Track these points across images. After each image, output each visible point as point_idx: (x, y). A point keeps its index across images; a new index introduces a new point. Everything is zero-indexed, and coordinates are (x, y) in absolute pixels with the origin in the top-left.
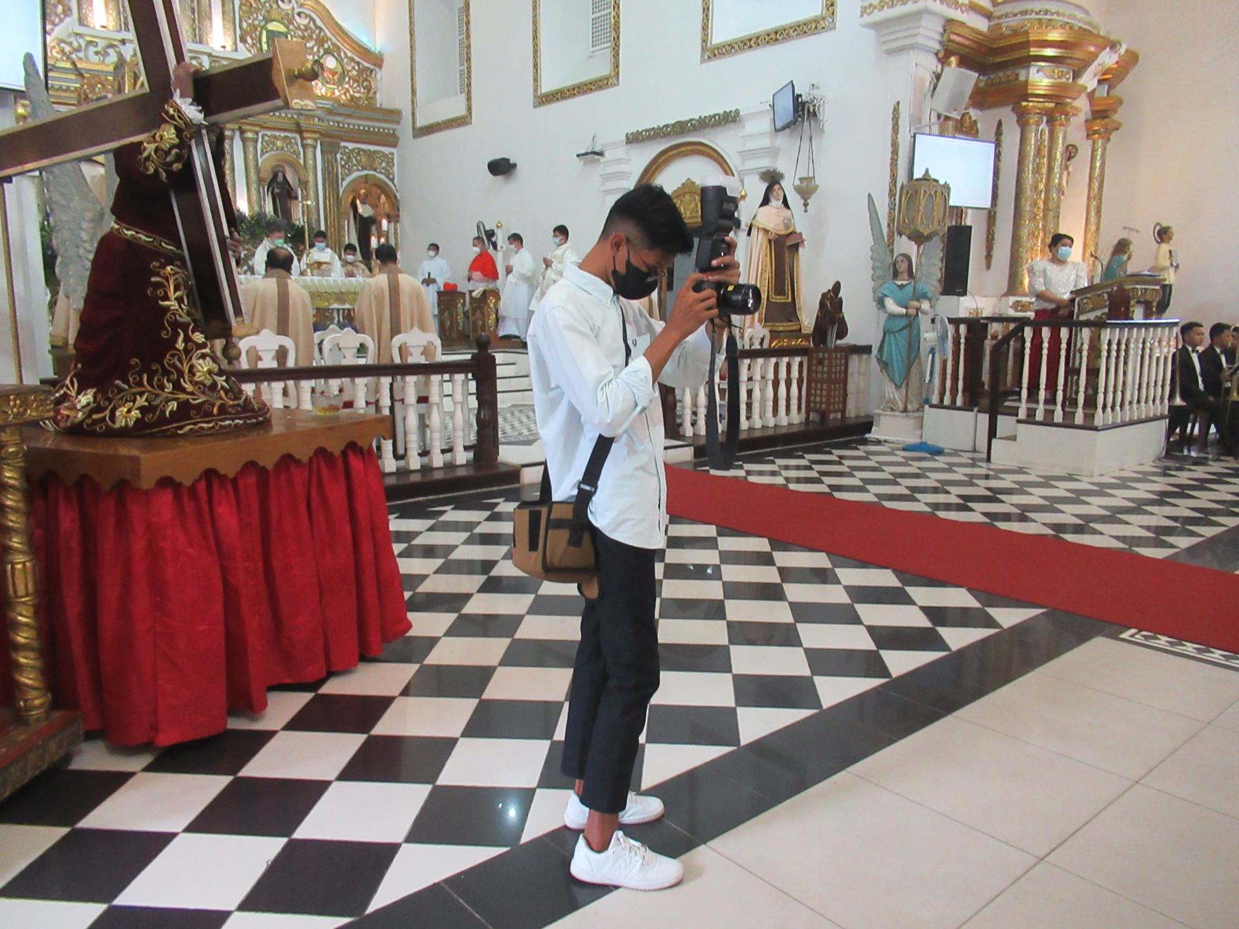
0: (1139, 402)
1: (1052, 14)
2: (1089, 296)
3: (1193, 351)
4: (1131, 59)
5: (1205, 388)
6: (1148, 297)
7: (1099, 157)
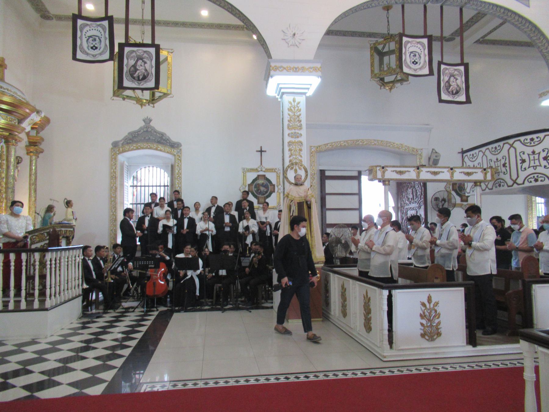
0: (68, 289)
1: (4, 89)
2: (36, 234)
3: (89, 260)
4: (46, 121)
5: (96, 277)
6: (68, 234)
7: (34, 164)
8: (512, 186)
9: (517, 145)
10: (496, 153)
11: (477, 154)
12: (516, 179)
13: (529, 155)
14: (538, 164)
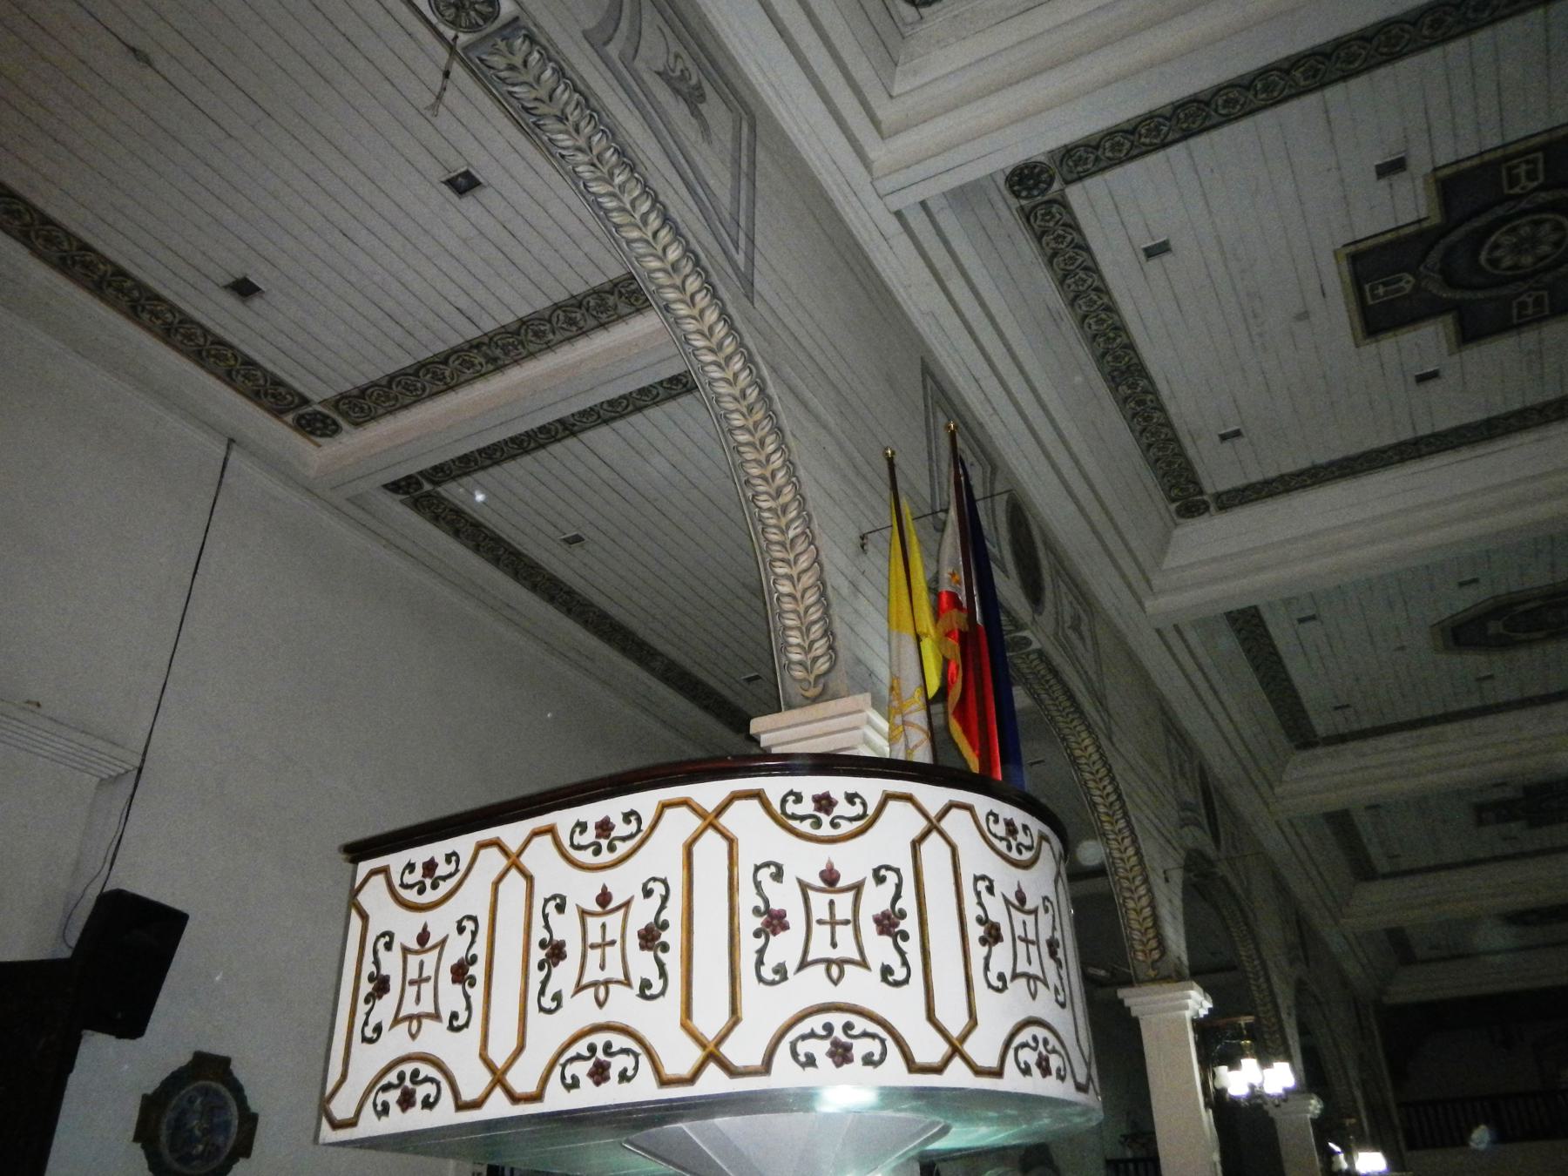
8: (692, 1080)
9: (745, 819)
10: (606, 857)
11: (463, 867)
12: (722, 1038)
13: (804, 887)
14: (857, 957)
